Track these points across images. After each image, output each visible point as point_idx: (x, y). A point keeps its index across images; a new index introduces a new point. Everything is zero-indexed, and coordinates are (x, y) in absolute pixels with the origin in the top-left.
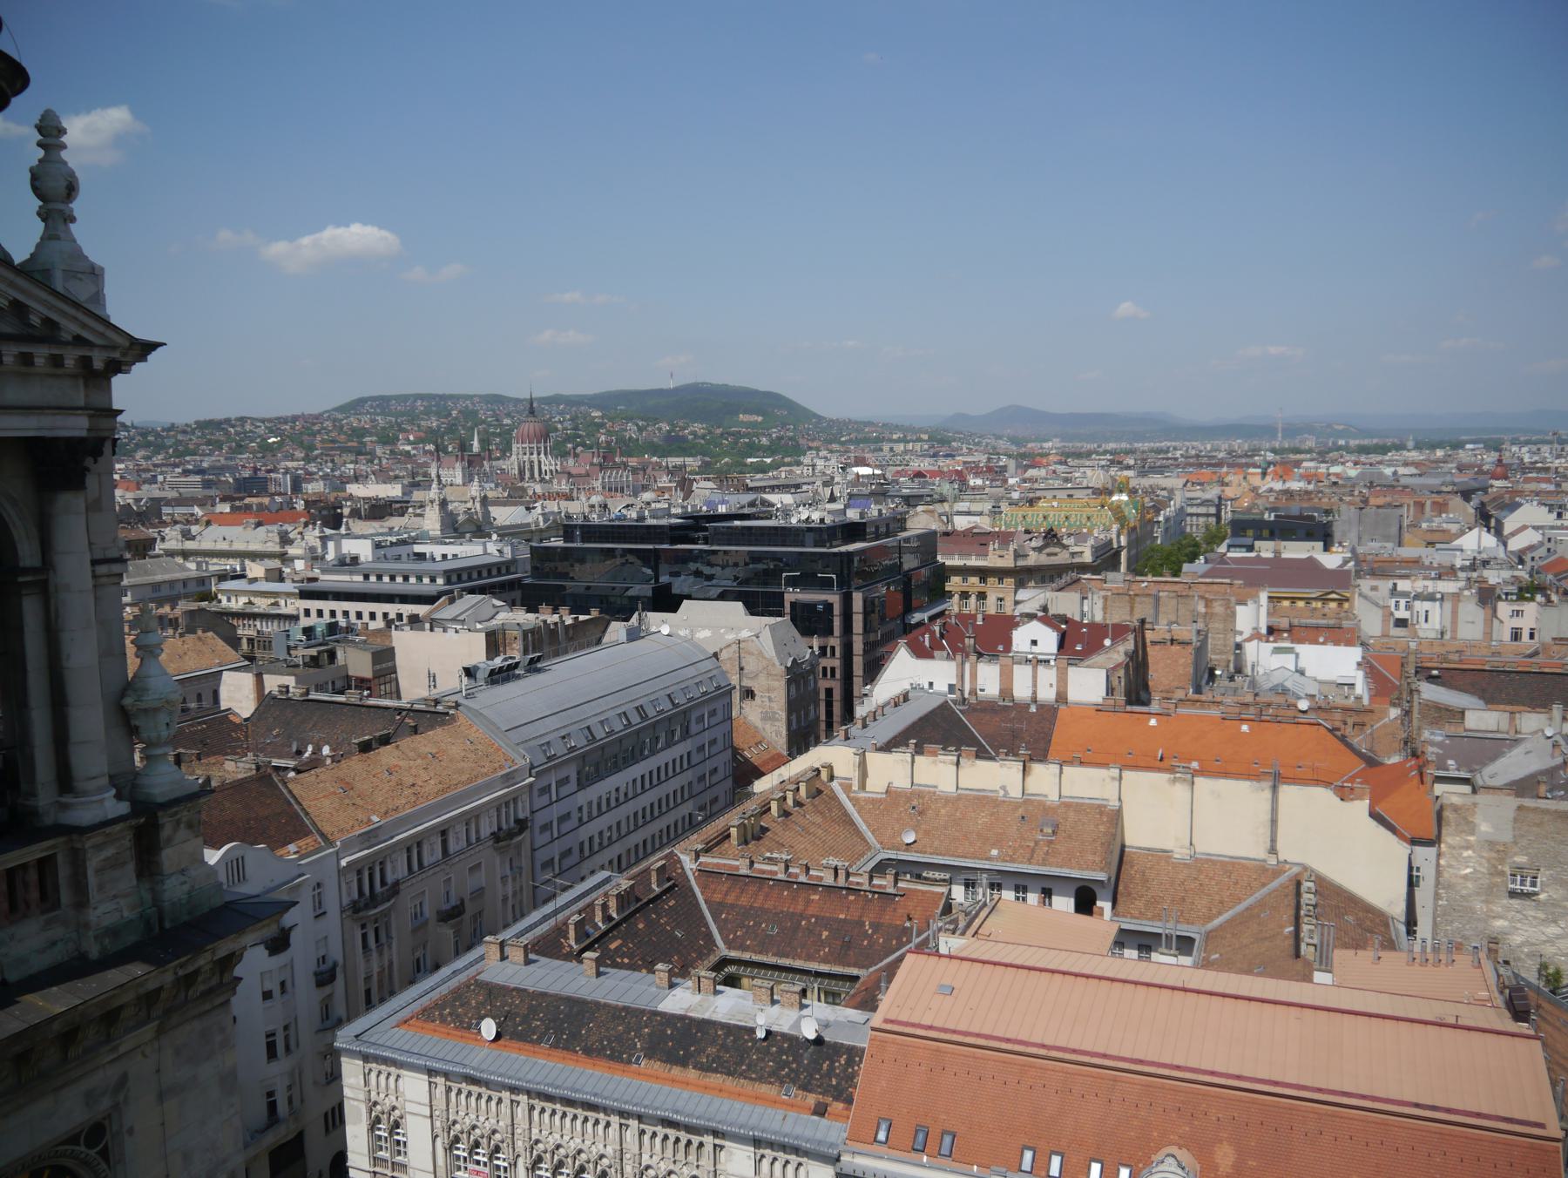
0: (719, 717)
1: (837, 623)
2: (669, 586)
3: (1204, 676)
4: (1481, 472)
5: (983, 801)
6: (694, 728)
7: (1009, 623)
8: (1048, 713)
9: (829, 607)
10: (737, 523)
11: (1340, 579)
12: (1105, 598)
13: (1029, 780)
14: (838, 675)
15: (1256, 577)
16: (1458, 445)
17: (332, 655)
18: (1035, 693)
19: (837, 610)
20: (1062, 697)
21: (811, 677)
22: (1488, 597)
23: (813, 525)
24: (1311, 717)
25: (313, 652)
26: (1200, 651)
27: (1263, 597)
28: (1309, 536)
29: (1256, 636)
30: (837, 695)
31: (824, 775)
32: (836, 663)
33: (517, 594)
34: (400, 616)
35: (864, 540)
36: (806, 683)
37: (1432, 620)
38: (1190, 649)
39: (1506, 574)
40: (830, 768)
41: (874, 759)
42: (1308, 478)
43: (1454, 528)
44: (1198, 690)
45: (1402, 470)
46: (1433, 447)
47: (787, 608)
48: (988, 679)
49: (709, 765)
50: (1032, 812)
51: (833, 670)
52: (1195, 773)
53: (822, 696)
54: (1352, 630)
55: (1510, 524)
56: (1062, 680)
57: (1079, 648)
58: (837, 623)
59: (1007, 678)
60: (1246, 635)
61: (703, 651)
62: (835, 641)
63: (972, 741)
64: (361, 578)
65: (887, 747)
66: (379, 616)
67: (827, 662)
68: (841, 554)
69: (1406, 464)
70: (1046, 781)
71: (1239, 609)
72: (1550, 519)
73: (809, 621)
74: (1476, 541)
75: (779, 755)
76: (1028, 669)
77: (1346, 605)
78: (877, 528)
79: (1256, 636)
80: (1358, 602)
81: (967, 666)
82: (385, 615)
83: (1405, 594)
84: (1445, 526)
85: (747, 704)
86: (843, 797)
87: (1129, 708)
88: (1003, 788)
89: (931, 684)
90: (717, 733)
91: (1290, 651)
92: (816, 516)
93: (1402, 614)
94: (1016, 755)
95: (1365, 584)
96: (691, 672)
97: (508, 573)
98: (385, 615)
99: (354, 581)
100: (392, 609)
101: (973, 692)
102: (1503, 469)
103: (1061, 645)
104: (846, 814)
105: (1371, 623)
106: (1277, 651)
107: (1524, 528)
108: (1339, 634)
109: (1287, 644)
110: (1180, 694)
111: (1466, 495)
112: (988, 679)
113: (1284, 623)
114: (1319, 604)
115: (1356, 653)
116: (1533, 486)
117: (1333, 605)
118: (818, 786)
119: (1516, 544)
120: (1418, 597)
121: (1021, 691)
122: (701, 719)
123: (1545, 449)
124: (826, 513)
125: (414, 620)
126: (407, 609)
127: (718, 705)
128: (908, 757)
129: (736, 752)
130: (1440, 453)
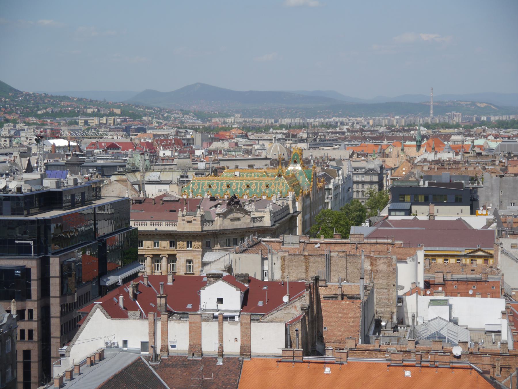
1: (34, 287)
9: (26, 272)
12: (283, 259)
14: (35, 337)
18: (221, 347)
19: (34, 274)
20: (246, 350)
21: (9, 340)
23: (10, 194)
24: (465, 362)
26: (367, 305)
27: (420, 255)
28: (458, 201)
29: (415, 290)
30: (35, 357)
32: (34, 325)
35: (60, 208)
38: (358, 303)
42: (456, 150)
44: (366, 340)
51: (31, 332)
53: (20, 358)
54: (496, 284)
56: (246, 335)
58: (34, 287)
60: (407, 289)
62: (32, 305)
67: (24, 325)
68: (38, 221)
71: (401, 266)
76: (215, 325)
77: (491, 261)
78: (73, 196)
79: (415, 290)
80: (501, 258)
81: (159, 324)
87: (306, 359)
89: (125, 342)
91: (444, 302)
92: (13, 185)
101: (165, 348)
103: (244, 303)
106: (433, 303)
109: (442, 297)
110: (350, 344)
113: (439, 278)
114: (468, 261)
115: (500, 304)
117: (480, 261)
124: (23, 183)
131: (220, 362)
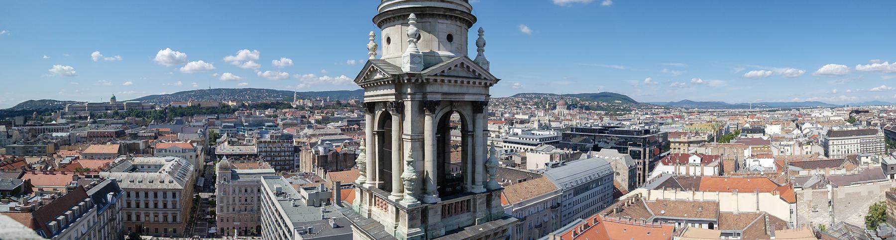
0: (610, 180)
2: (597, 145)
3: (737, 167)
4: (796, 116)
5: (682, 202)
6: (604, 182)
7: (689, 156)
8: (699, 178)
10: (616, 129)
11: (767, 142)
13: (694, 196)
15: (748, 143)
16: (790, 110)
17: (511, 157)
22: (800, 145)
24: (765, 176)
25: (507, 156)
26: (736, 161)
27: (750, 147)
28: (760, 132)
29: (749, 157)
31: (639, 196)
33: (558, 145)
34: (527, 149)
36: (634, 172)
37: (789, 151)
38: (734, 161)
39: (804, 139)
40: (641, 194)
41: (652, 191)
42: (758, 118)
43: (791, 129)
44: (736, 172)
45: (779, 116)
46: (785, 110)
47: (629, 152)
48: (683, 170)
49: (607, 192)
50: (696, 204)
52: (738, 192)
54: (771, 154)
55: (803, 127)
56: (702, 170)
57: (706, 161)
59: (688, 170)
60: (747, 157)
61: (607, 162)
63: (680, 187)
64: (518, 138)
65: (657, 189)
66: (522, 149)
69: (780, 114)
70: (700, 196)
71: (745, 151)
72: (811, 126)
73: (635, 155)
74: (797, 132)
75: (626, 190)
76: (694, 167)
77: (769, 149)
79: (749, 157)
80: (772, 148)
82: (524, 149)
83: (783, 145)
84: (790, 129)
85: (618, 176)
86: (644, 202)
88: (688, 198)
90: (610, 184)
92: (637, 128)
93: (782, 150)
94: (691, 190)
95: (774, 143)
96: (604, 167)
97: (556, 139)
98: (524, 149)
99: (516, 139)
100: (526, 147)
102: (801, 115)
104: (645, 206)
105: (775, 152)
106: (754, 161)
107: (806, 128)
108: (769, 156)
109: (757, 159)
110: (732, 173)
111: (793, 121)
112: (683, 170)
113: (755, 154)
114: (763, 149)
115: (773, 160)
116: (807, 119)
117: (766, 149)
118: (638, 199)
119: (805, 132)
120: (785, 146)
121: (691, 173)
122: (605, 180)
123: (808, 110)
125: (532, 150)
126: (530, 147)
127: (610, 177)
128: (663, 191)
129: (614, 188)
130: (787, 111)
131: (695, 178)
